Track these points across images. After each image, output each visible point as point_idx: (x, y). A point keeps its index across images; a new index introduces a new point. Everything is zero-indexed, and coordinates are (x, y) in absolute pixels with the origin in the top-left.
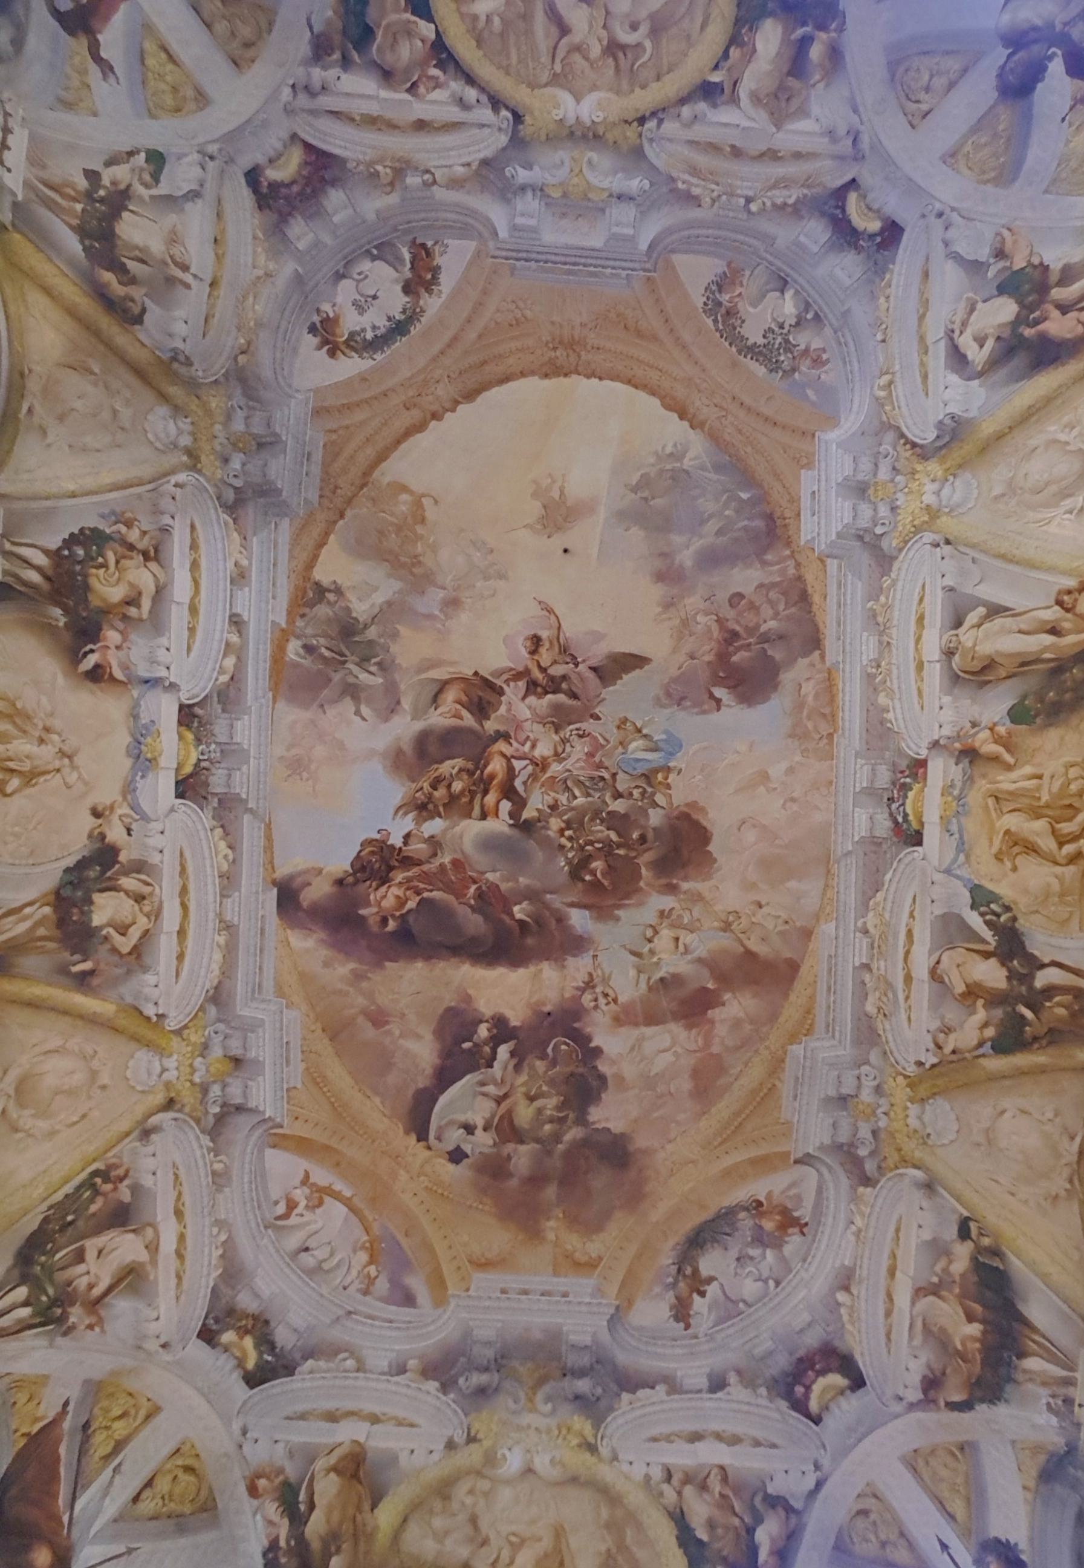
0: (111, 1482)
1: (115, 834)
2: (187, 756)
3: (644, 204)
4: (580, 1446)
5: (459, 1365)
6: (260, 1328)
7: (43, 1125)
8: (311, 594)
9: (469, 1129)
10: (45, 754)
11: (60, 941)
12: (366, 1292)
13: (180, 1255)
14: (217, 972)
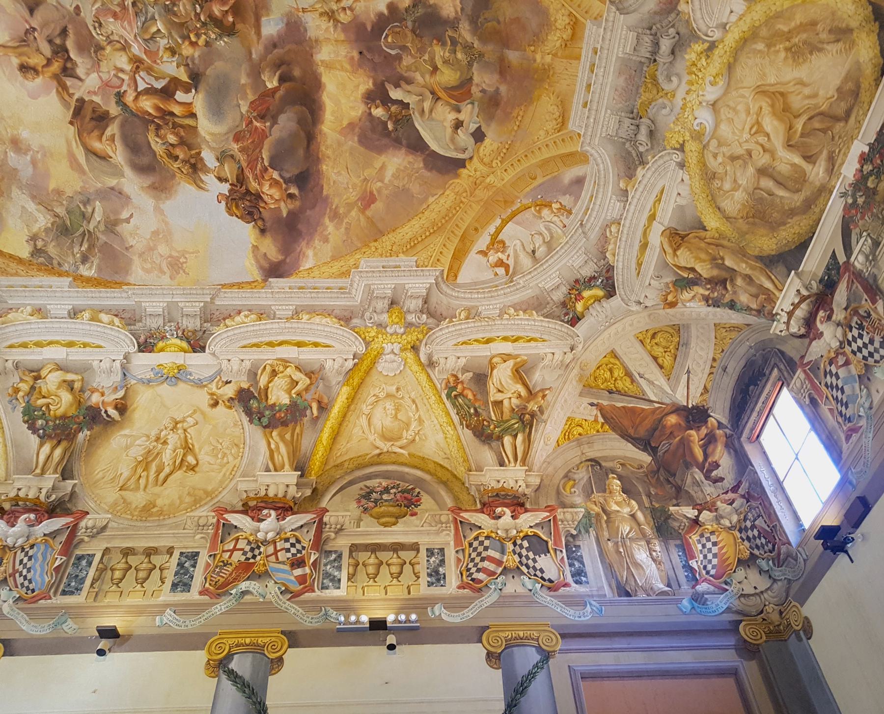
0: (648, 380)
1: (229, 391)
2: (175, 345)
4: (708, 57)
5: (630, 149)
6: (578, 286)
7: (414, 425)
9: (458, 124)
10: (174, 439)
11: (296, 423)
12: (570, 212)
13: (517, 340)
14: (328, 320)
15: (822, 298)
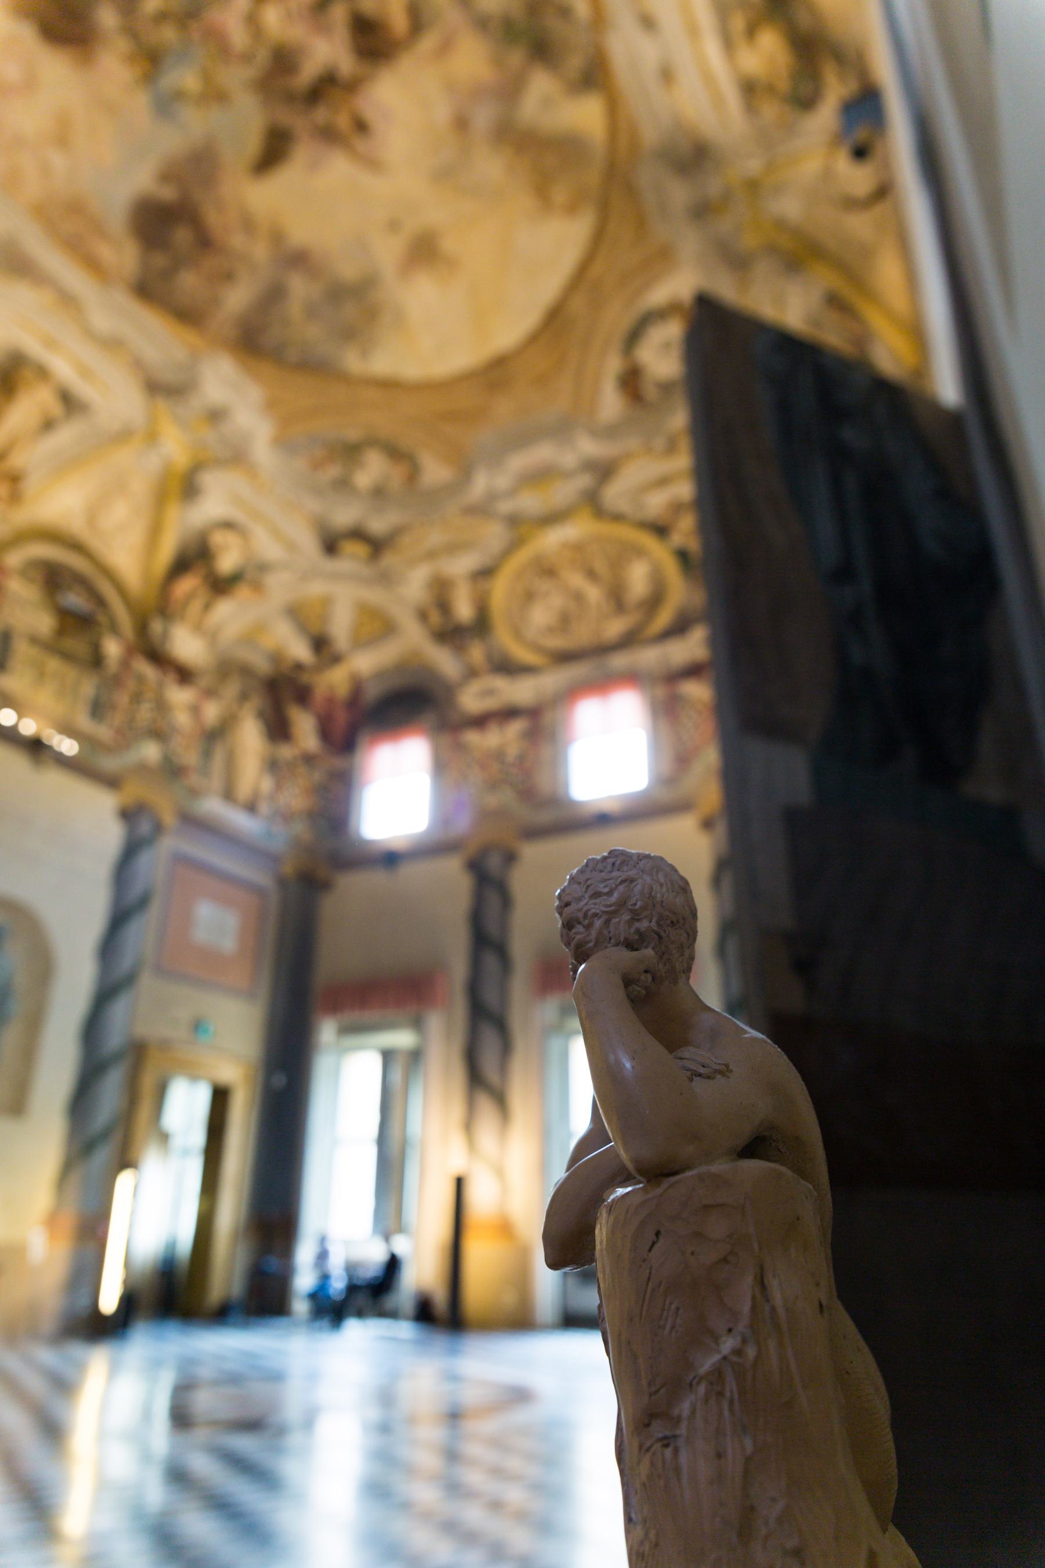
3: (492, 497)
8: (595, 77)
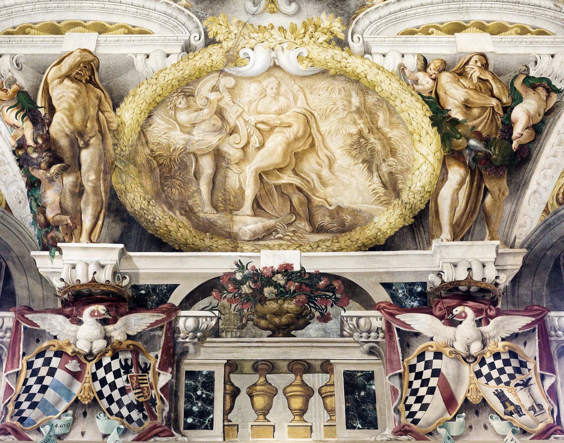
4: (329, 42)
15: (120, 299)
